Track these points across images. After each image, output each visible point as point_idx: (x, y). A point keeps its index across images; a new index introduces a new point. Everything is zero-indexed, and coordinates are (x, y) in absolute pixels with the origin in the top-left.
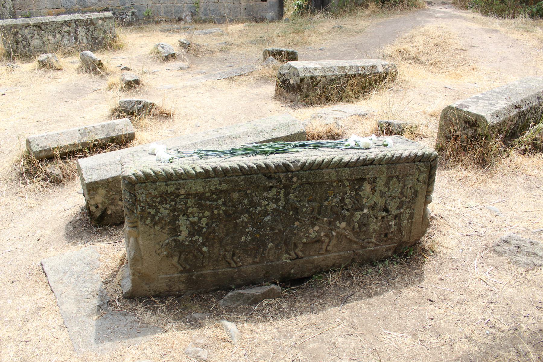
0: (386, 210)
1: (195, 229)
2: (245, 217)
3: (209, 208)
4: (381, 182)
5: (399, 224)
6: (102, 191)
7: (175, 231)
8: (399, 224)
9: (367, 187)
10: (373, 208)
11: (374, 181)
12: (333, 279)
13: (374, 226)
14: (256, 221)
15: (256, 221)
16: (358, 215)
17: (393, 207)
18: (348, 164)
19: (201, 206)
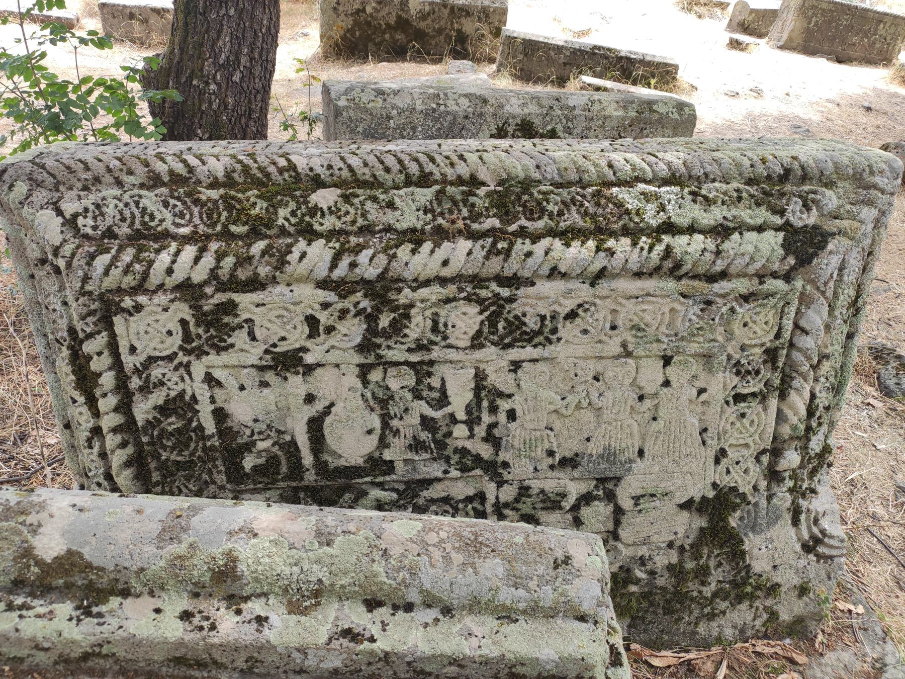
0: (885, 39)
1: (816, 24)
2: (834, 24)
3: (825, 16)
4: (888, 25)
5: (888, 48)
6: (754, 15)
7: (809, 23)
8: (888, 48)
9: (882, 25)
10: (880, 36)
11: (885, 23)
12: (854, 63)
13: (878, 45)
14: (837, 28)
15: (837, 28)
16: (874, 37)
17: (888, 38)
18: (878, 13)
19: (822, 15)
